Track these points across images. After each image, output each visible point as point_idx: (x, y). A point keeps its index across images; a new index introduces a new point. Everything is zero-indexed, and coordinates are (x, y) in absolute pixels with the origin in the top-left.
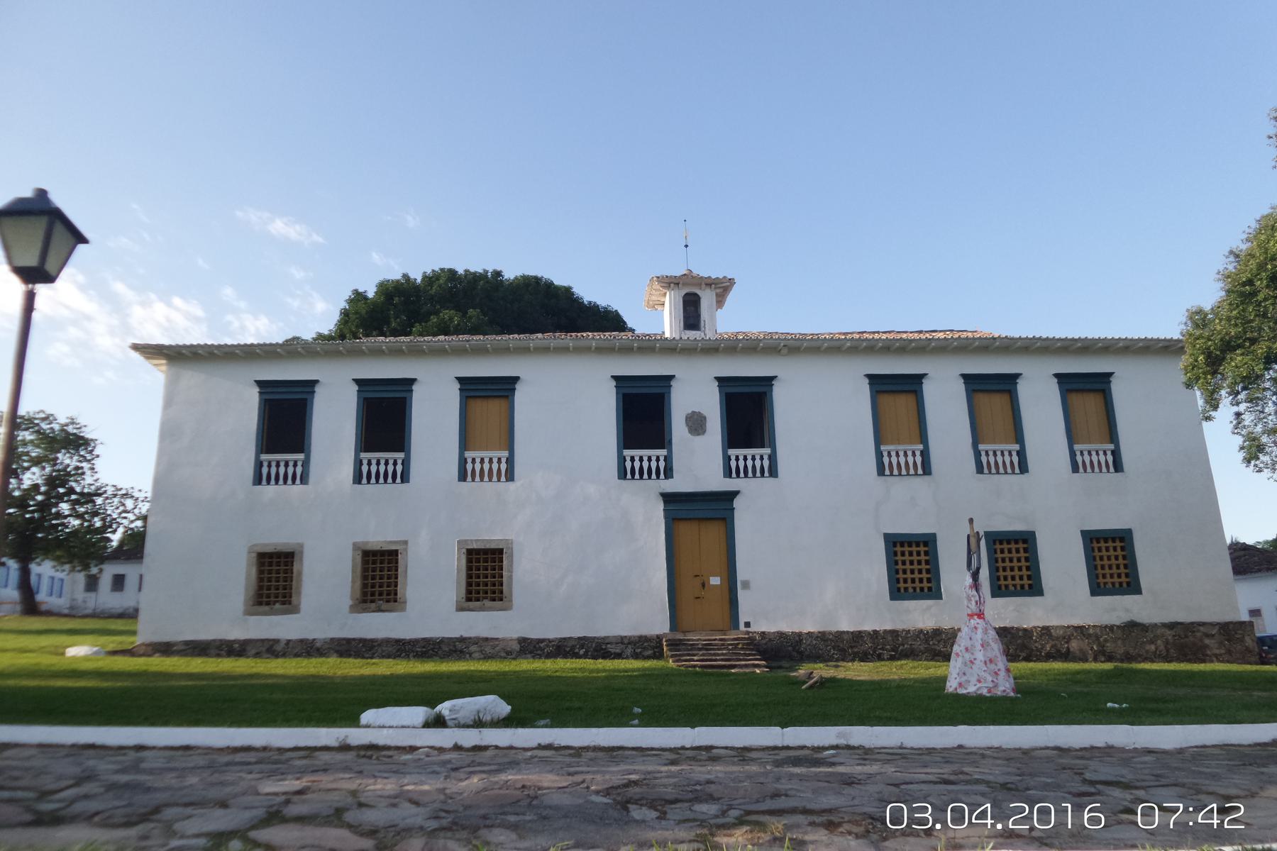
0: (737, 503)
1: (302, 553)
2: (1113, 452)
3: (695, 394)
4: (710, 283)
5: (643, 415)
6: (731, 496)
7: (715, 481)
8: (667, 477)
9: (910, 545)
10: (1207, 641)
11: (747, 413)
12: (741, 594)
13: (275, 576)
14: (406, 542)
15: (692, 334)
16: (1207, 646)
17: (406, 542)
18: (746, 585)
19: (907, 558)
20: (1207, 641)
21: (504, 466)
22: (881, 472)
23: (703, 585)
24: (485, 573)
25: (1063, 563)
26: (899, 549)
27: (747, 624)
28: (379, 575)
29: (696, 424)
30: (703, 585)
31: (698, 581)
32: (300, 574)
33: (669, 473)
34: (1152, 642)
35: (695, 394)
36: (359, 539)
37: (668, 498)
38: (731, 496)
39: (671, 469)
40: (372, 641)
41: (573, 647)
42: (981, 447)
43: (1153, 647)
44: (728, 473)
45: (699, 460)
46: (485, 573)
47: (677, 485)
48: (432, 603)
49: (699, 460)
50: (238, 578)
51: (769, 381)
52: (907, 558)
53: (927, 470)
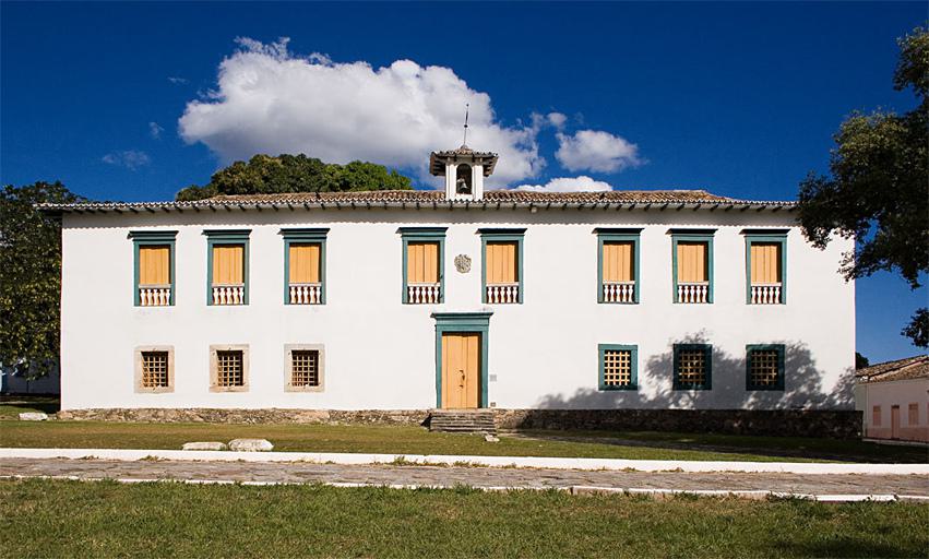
1: (173, 351)
2: (780, 289)
4: (475, 158)
6: (487, 316)
7: (477, 306)
8: (439, 302)
9: (618, 352)
10: (825, 423)
12: (491, 385)
13: (157, 364)
14: (248, 346)
15: (464, 197)
16: (825, 427)
17: (248, 346)
18: (494, 378)
19: (615, 361)
20: (825, 423)
23: (463, 377)
24: (307, 365)
26: (609, 355)
27: (493, 404)
28: (231, 365)
29: (462, 264)
30: (463, 377)
31: (461, 375)
33: (440, 299)
34: (785, 422)
38: (487, 316)
39: (443, 296)
40: (225, 411)
41: (367, 417)
43: (785, 426)
46: (307, 365)
48: (269, 386)
50: (136, 366)
52: (615, 361)
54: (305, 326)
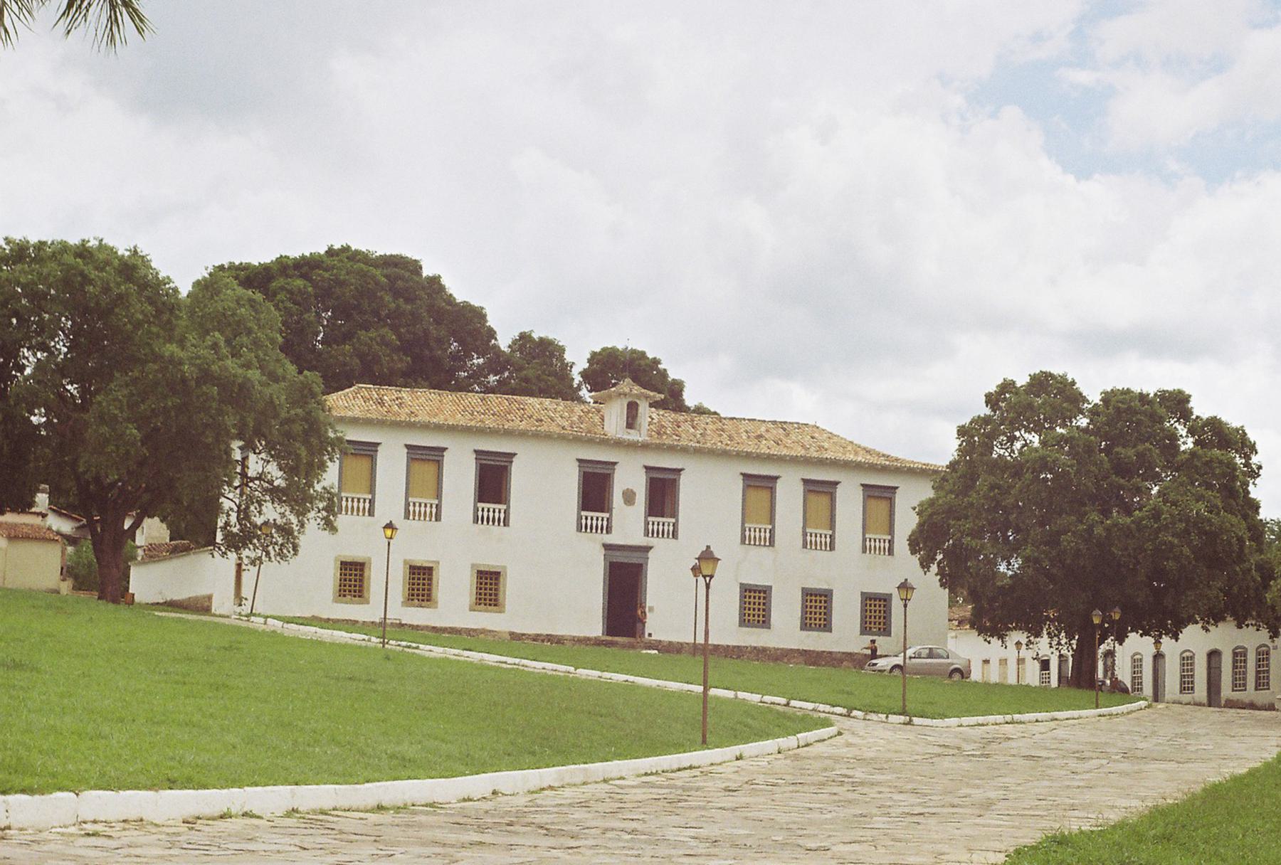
0: (651, 554)
3: (630, 478)
5: (595, 491)
6: (647, 549)
7: (638, 539)
11: (662, 494)
18: (651, 609)
21: (502, 516)
22: (743, 542)
24: (488, 586)
25: (846, 613)
28: (421, 582)
32: (369, 578)
35: (630, 478)
36: (408, 557)
37: (607, 547)
38: (647, 549)
42: (808, 530)
44: (647, 534)
45: (629, 523)
46: (488, 586)
47: (615, 538)
49: (629, 523)
51: (678, 471)
53: (772, 544)
54: (491, 547)
